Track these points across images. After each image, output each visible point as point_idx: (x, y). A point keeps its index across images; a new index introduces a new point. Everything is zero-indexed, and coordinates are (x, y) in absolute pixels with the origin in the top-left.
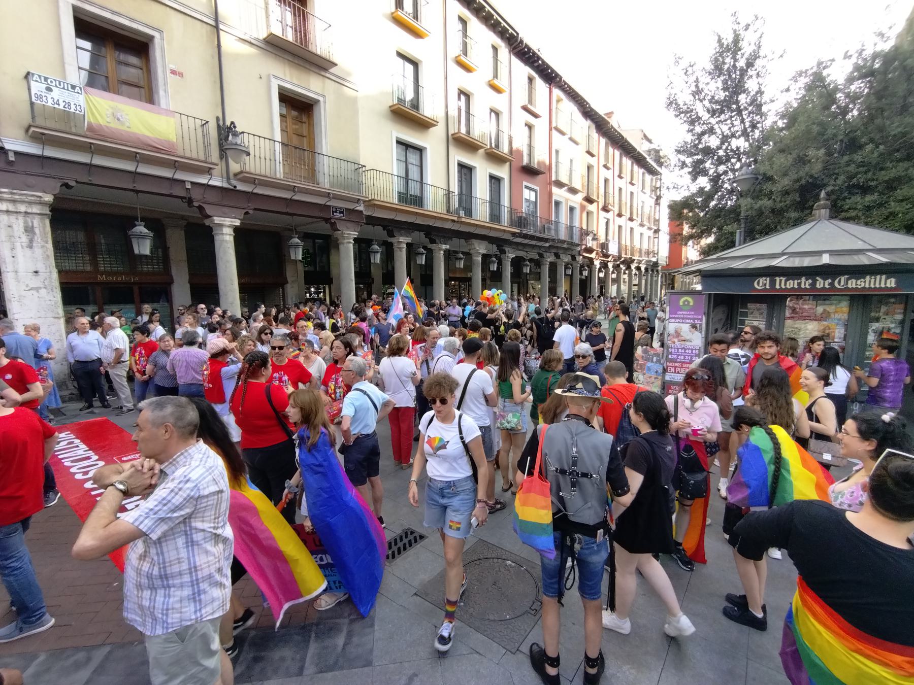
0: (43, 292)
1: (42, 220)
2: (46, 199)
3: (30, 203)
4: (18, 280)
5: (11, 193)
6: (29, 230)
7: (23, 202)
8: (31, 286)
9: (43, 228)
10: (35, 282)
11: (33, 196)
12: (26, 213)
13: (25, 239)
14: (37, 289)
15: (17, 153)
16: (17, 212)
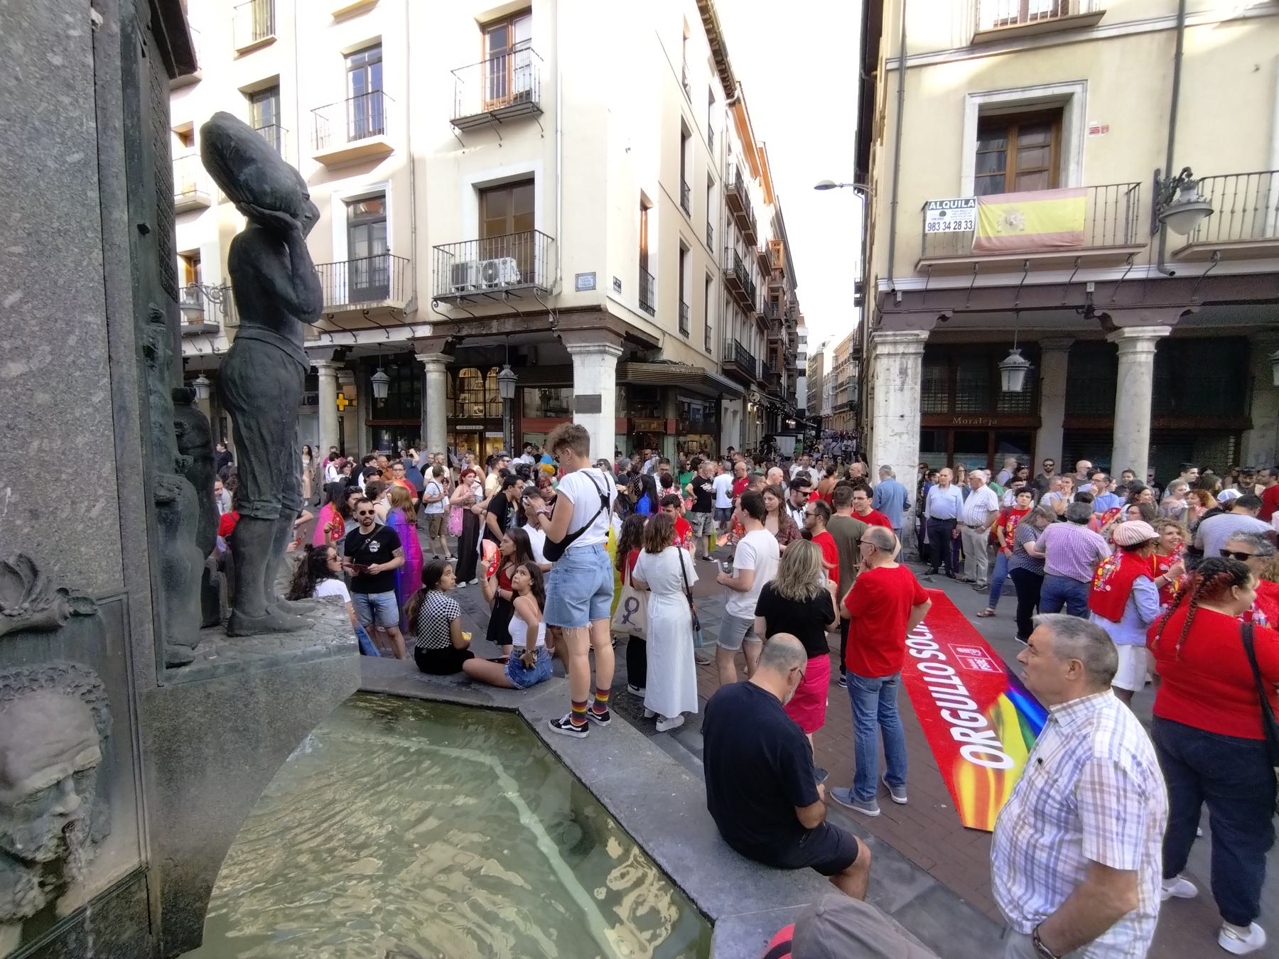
0: (905, 437)
1: (916, 359)
2: (923, 337)
3: (908, 343)
4: (886, 425)
5: (894, 335)
6: (903, 372)
7: (902, 342)
8: (896, 431)
9: (915, 367)
10: (900, 427)
11: (912, 335)
12: (904, 354)
13: (898, 382)
14: (900, 434)
15: (905, 292)
16: (895, 354)
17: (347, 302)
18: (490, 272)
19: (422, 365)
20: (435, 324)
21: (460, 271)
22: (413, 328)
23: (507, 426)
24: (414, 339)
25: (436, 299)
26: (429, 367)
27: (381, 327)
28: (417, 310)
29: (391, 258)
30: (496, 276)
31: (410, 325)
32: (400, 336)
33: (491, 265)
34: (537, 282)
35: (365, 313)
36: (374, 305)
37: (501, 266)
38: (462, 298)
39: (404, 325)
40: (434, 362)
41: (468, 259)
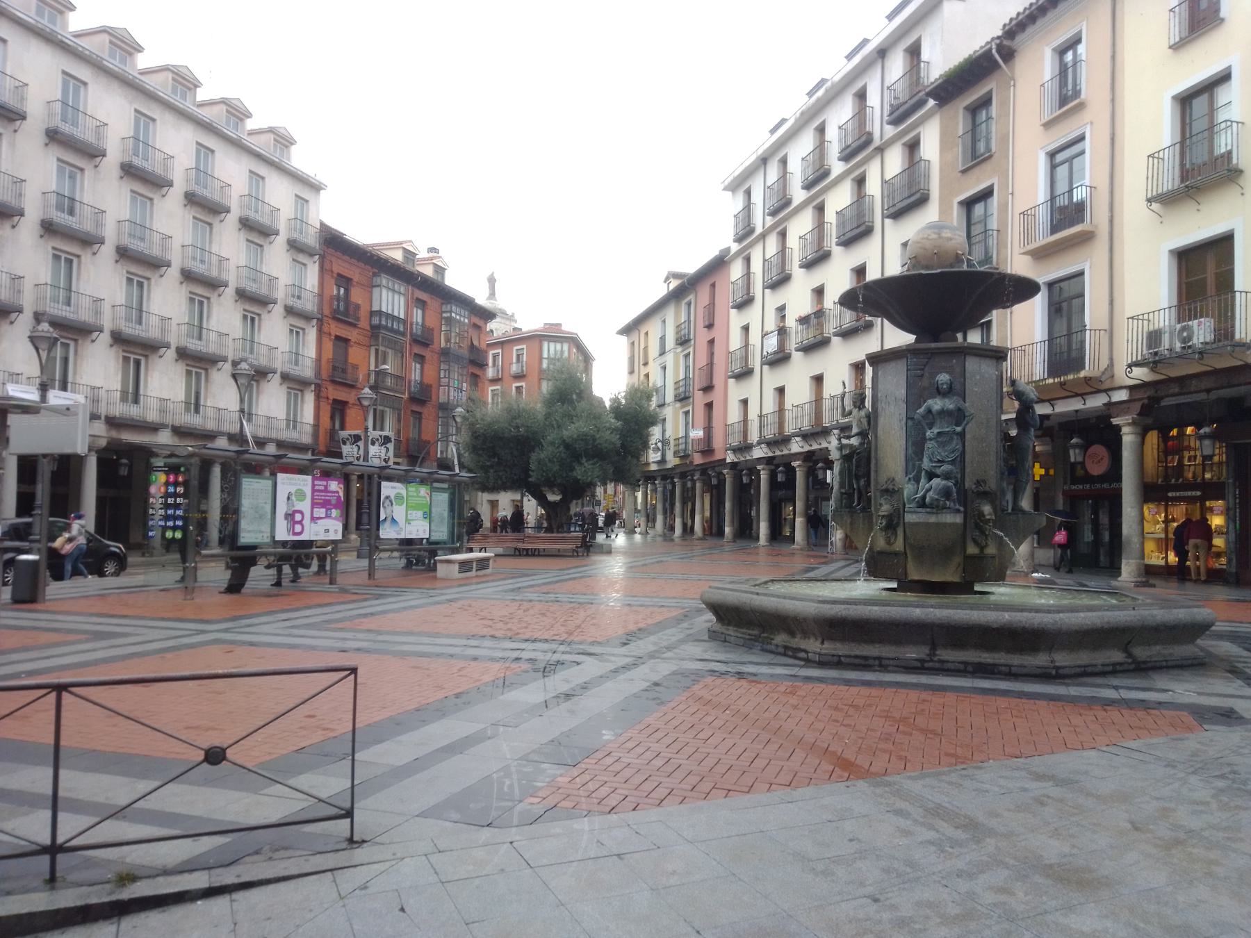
17: (1046, 376)
18: (1185, 334)
19: (1118, 429)
20: (1131, 388)
21: (1154, 337)
22: (1109, 393)
23: (1231, 492)
24: (1109, 405)
25: (1130, 366)
26: (1125, 430)
27: (1077, 395)
28: (1113, 376)
29: (1088, 332)
30: (1190, 338)
31: (1106, 391)
32: (1096, 402)
33: (1184, 329)
34: (1237, 336)
35: (1062, 384)
36: (1070, 377)
37: (1195, 328)
38: (1155, 362)
39: (1099, 391)
40: (1129, 424)
41: (1162, 325)
